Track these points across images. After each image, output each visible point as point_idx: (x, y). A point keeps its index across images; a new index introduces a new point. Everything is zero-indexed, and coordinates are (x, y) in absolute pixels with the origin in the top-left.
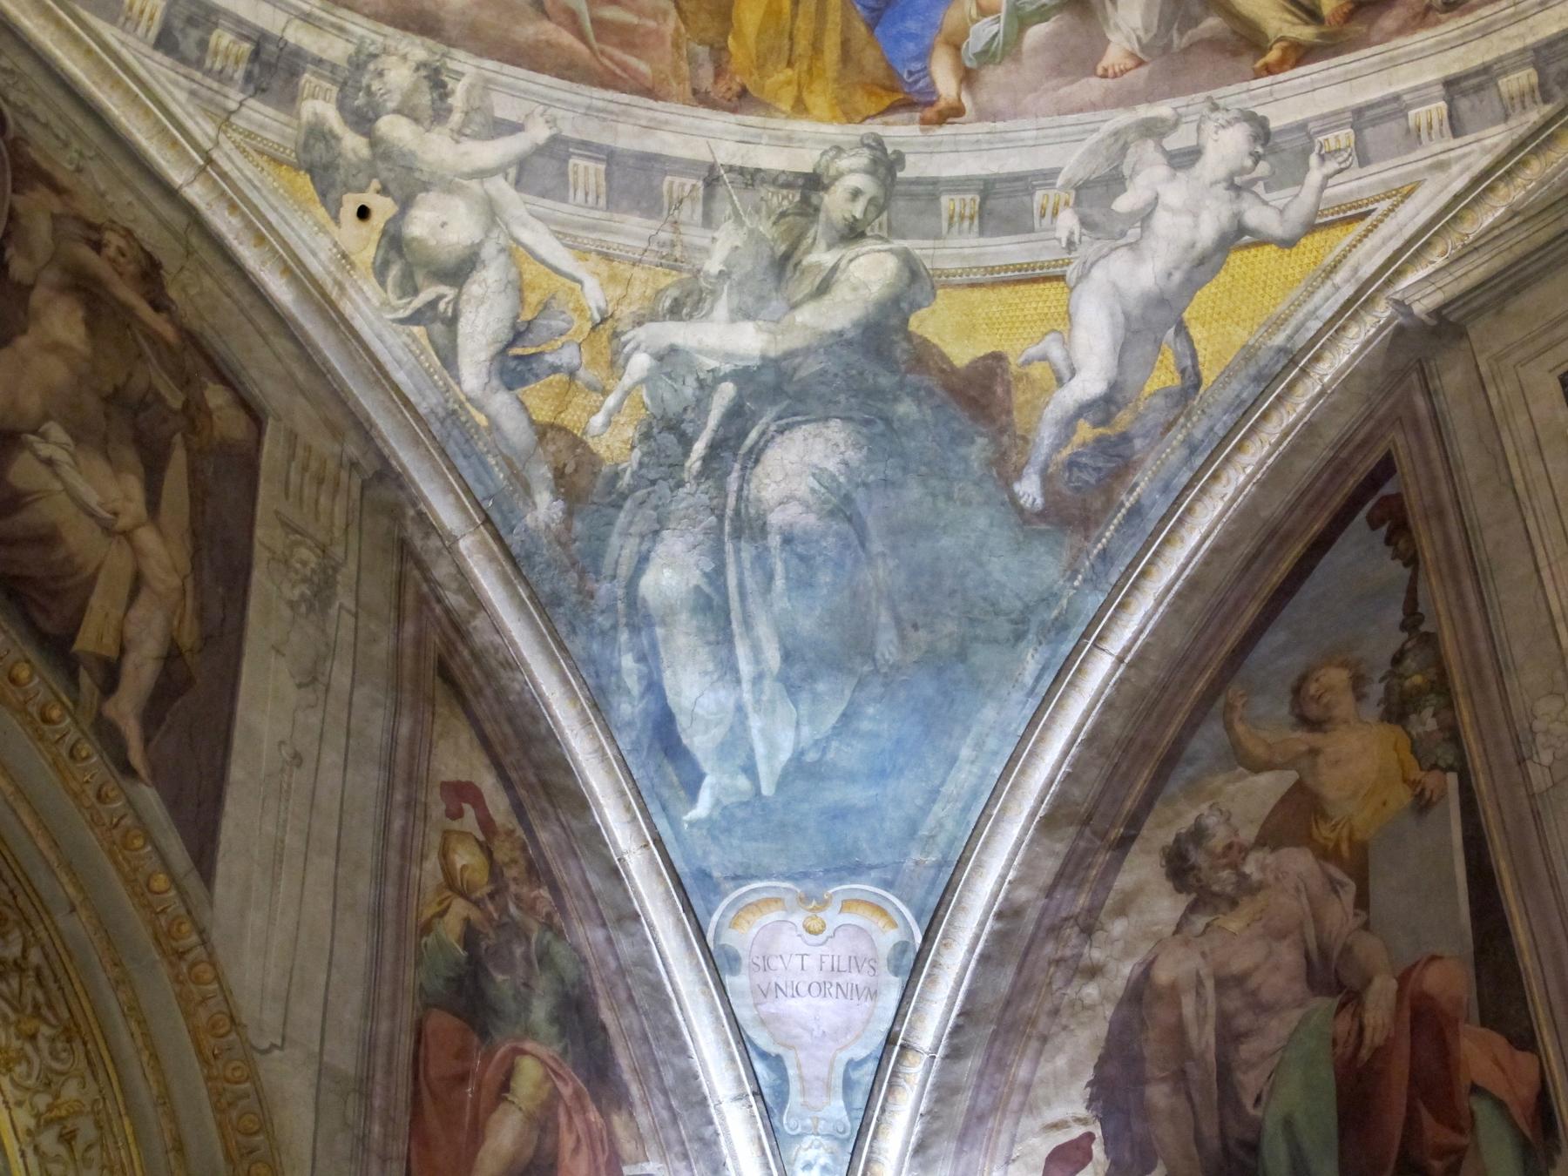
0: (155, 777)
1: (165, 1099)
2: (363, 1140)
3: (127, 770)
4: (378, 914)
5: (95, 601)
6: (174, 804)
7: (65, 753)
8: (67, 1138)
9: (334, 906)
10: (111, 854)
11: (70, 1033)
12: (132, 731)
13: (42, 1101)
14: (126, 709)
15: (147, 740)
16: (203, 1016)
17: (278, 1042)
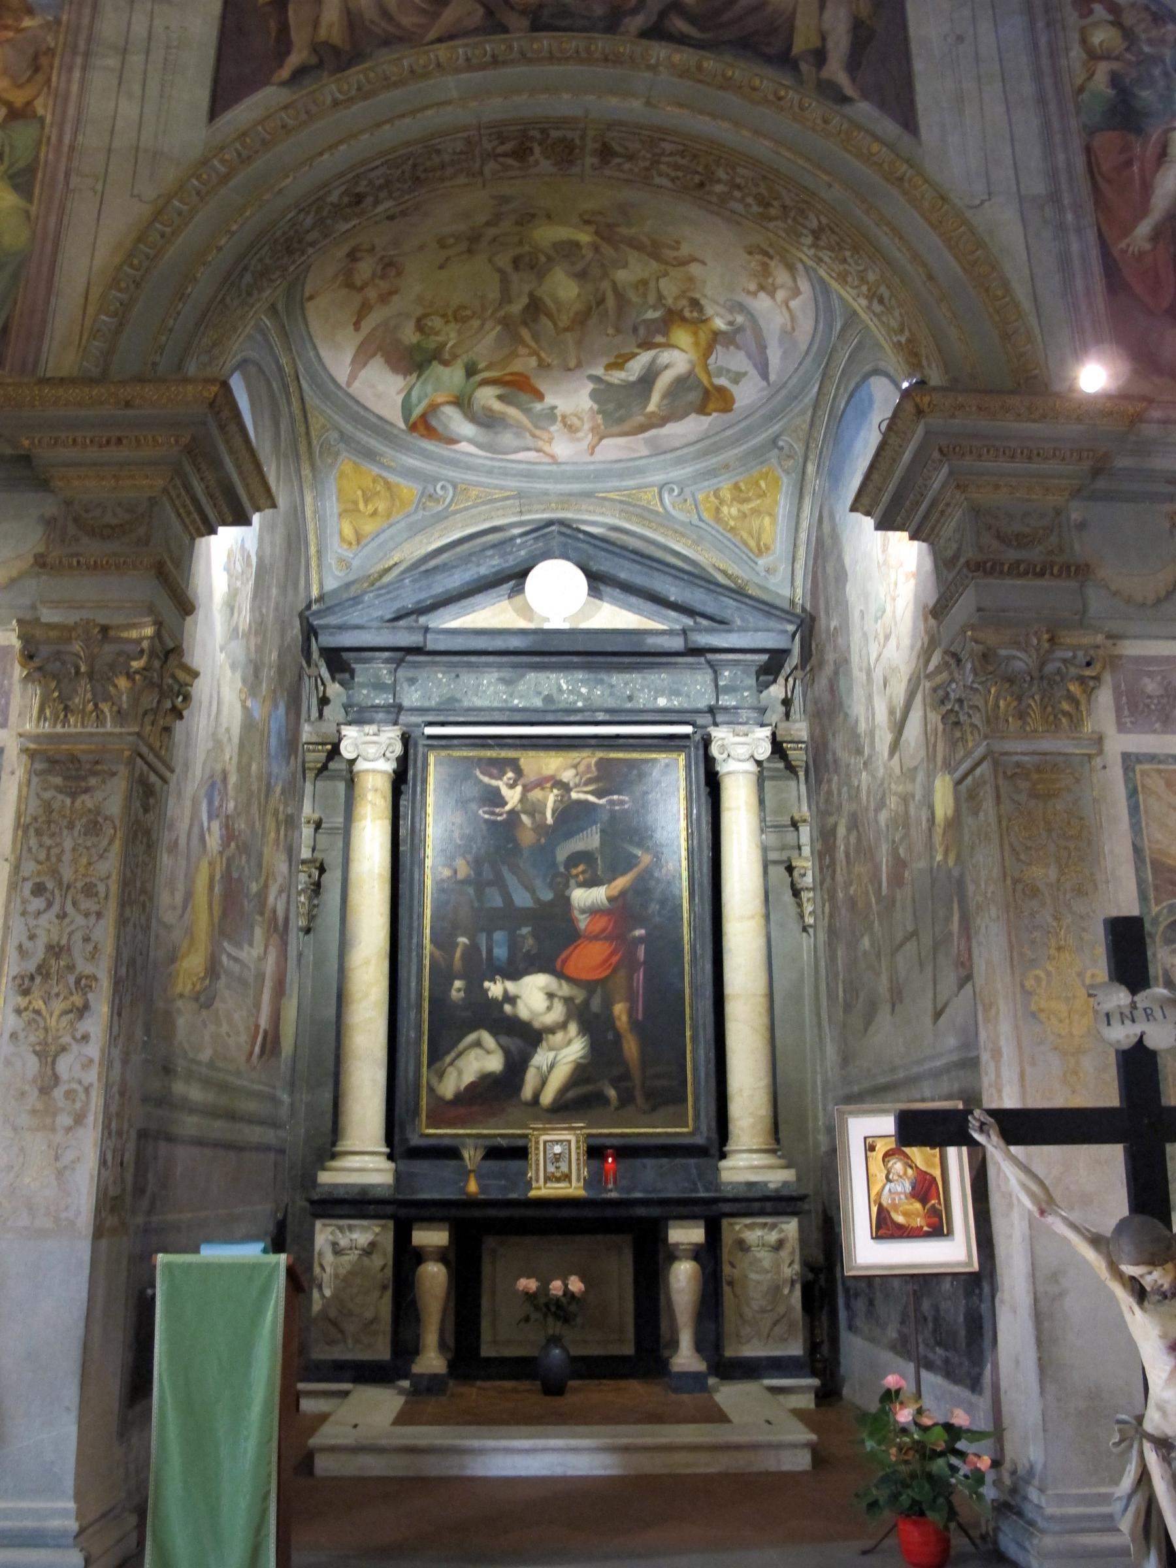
0: (865, 96)
1: (916, 257)
2: (1061, 227)
3: (845, 100)
4: (1042, 100)
5: (799, 23)
6: (882, 104)
7: (797, 110)
8: (881, 301)
9: (1008, 110)
10: (845, 149)
11: (856, 249)
12: (842, 79)
13: (864, 288)
14: (836, 70)
15: (853, 80)
16: (926, 204)
17: (986, 197)
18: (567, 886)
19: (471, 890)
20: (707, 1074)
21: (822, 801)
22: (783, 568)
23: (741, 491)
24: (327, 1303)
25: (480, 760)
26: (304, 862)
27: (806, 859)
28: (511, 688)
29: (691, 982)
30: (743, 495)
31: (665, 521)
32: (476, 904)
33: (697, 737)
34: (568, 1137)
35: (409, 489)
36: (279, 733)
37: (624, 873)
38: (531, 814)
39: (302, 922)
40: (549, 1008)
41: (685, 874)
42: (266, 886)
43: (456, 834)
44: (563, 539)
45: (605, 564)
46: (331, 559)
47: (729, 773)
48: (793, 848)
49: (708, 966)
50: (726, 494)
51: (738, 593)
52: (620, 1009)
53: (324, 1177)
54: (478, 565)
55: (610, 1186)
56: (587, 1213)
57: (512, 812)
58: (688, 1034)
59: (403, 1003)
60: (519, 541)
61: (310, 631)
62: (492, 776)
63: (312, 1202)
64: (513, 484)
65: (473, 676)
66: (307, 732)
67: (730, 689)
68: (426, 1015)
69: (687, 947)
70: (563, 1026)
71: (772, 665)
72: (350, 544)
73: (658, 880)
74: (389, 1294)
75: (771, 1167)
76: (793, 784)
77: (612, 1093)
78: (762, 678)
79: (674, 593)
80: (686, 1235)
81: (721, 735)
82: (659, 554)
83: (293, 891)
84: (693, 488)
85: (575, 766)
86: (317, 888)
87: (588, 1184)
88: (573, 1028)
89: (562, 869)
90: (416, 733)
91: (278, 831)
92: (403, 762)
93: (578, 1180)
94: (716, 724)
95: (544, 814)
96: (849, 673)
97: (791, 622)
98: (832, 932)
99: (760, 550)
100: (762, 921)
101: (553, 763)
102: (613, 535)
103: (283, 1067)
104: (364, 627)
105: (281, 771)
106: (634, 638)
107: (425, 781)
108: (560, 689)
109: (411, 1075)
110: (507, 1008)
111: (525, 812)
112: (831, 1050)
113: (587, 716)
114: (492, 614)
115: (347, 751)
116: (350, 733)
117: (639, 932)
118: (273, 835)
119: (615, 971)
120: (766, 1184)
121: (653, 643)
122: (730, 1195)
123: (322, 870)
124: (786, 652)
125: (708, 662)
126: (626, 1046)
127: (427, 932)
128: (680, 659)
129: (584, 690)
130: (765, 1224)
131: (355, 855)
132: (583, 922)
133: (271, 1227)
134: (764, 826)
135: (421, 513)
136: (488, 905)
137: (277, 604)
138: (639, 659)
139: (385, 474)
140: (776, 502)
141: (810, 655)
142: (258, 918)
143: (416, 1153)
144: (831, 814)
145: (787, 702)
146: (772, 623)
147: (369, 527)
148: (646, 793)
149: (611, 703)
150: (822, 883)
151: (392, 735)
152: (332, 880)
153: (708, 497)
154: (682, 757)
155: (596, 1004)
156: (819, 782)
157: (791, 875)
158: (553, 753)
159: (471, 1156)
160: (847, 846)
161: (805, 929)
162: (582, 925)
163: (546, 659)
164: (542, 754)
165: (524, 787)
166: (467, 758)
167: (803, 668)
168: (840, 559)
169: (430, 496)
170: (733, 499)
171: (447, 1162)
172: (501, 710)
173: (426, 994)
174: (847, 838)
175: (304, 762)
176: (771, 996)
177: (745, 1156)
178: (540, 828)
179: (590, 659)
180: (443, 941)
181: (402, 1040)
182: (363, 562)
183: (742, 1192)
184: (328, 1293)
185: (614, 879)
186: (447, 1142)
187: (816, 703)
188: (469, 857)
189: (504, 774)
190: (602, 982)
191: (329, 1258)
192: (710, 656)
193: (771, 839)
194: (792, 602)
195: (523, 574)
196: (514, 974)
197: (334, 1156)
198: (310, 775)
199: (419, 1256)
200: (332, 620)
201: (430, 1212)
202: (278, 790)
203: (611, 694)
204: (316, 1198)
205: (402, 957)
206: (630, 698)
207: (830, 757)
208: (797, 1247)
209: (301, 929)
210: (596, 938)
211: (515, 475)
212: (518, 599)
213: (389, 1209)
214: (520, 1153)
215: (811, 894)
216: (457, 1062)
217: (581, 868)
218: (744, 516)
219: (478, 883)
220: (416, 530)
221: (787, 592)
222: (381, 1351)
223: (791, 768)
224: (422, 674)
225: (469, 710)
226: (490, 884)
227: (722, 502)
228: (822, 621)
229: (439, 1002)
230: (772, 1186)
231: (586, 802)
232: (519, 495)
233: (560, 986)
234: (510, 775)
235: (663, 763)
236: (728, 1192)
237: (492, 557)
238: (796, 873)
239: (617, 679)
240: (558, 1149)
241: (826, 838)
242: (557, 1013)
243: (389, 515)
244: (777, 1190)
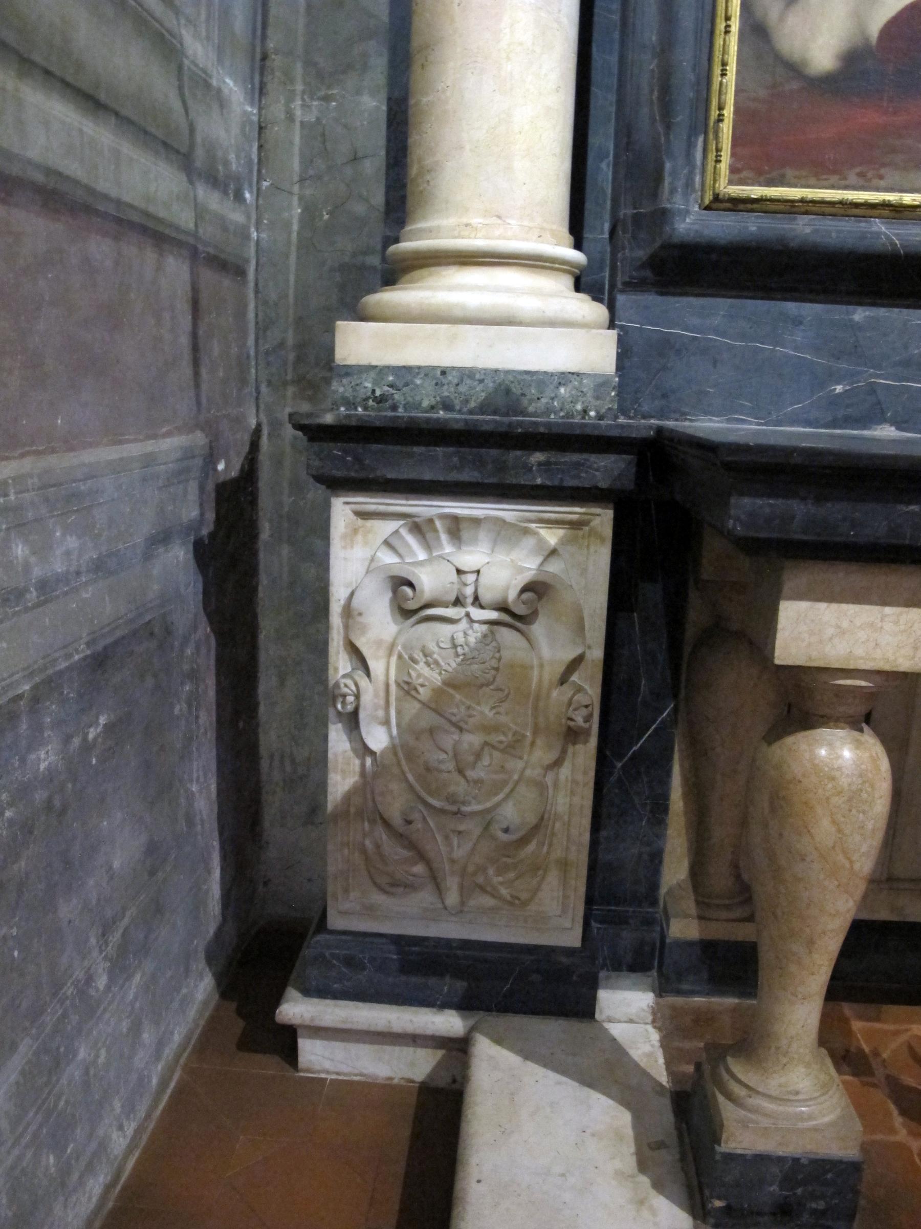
24: (376, 773)
53: (361, 344)
63: (316, 433)
74: (585, 755)
133: (192, 509)
143: (687, 269)
171: (792, 307)
184: (378, 738)
191: (380, 625)
197: (393, 273)
204: (329, 419)
213: (605, 469)
222: (555, 918)
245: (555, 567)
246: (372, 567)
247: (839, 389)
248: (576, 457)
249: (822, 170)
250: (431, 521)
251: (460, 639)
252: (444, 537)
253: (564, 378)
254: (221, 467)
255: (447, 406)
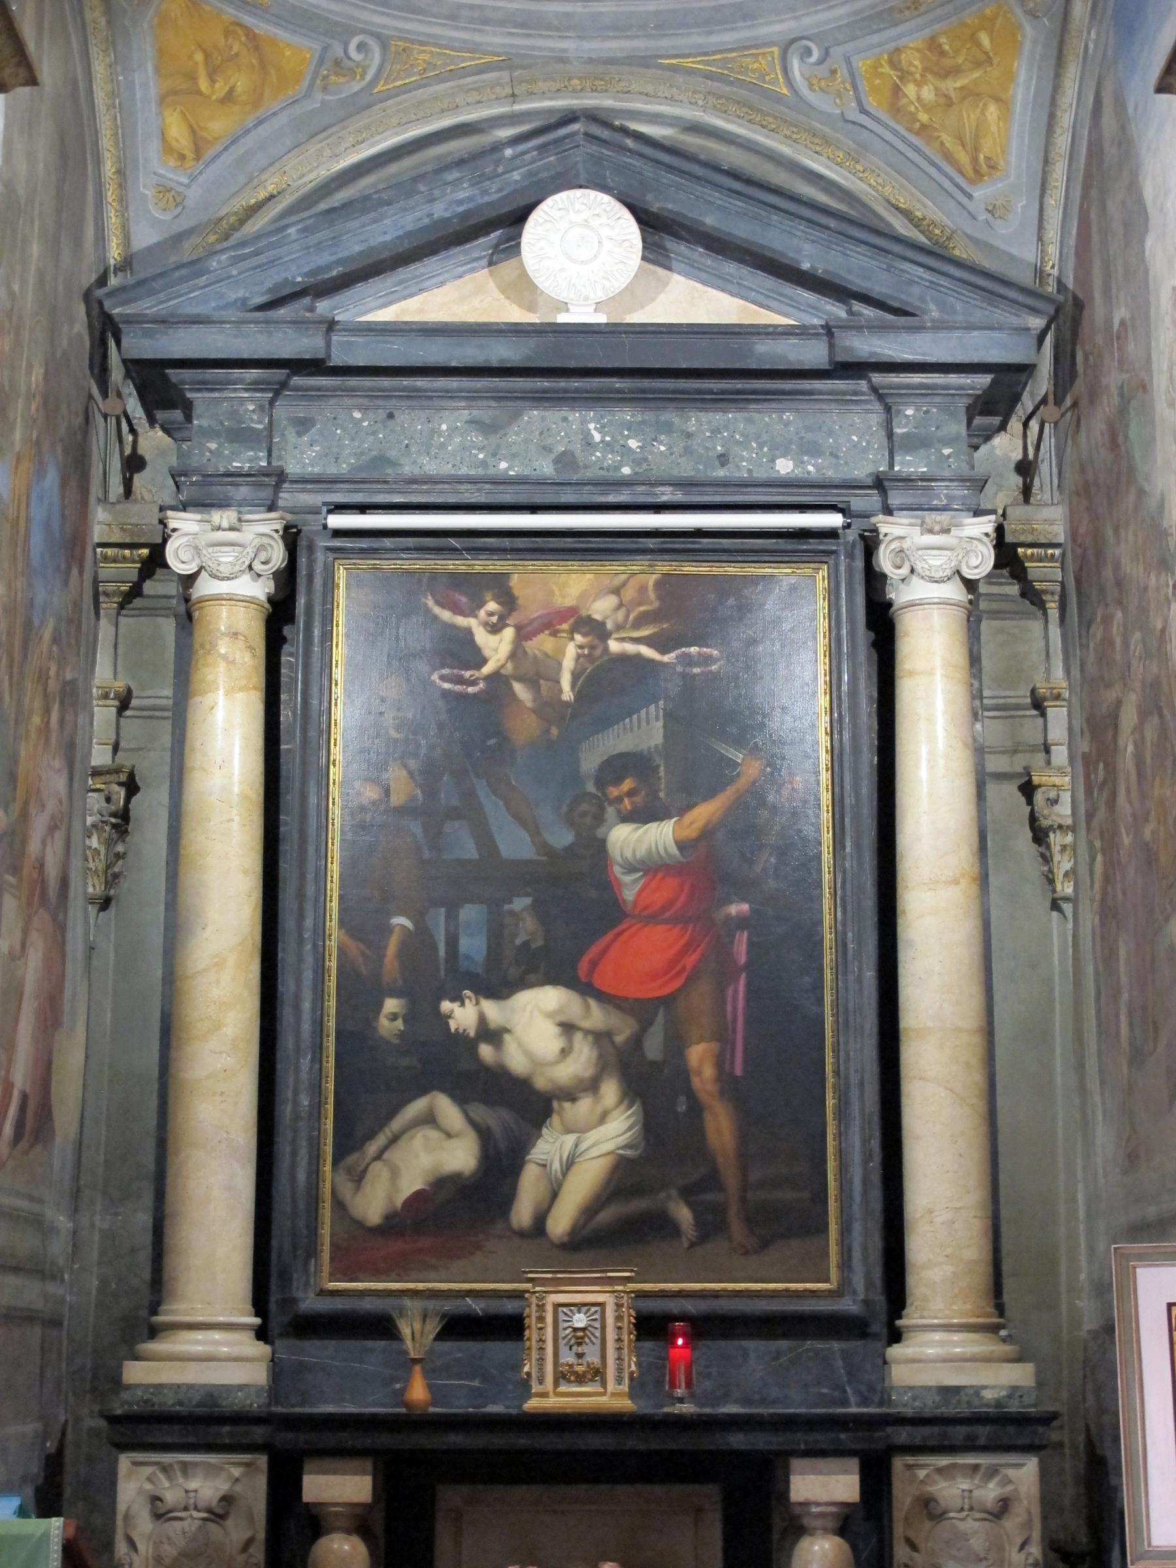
18: (599, 819)
19: (416, 827)
20: (865, 1181)
21: (1091, 657)
22: (1023, 205)
23: (943, 53)
25: (434, 576)
26: (96, 773)
27: (1061, 771)
28: (494, 439)
29: (836, 1004)
30: (947, 62)
31: (792, 114)
32: (427, 854)
33: (852, 536)
34: (600, 1298)
35: (296, 49)
36: (47, 524)
37: (711, 794)
38: (532, 682)
39: (95, 887)
40: (565, 1052)
41: (826, 798)
42: (24, 816)
43: (389, 720)
44: (594, 148)
45: (672, 200)
46: (145, 187)
47: (912, 605)
48: (1033, 749)
49: (870, 975)
50: (913, 60)
51: (934, 253)
52: (700, 1056)
53: (136, 1373)
54: (432, 200)
55: (680, 1392)
56: (633, 1442)
57: (496, 677)
58: (830, 1102)
59: (286, 1042)
60: (508, 152)
61: (106, 328)
62: (457, 610)
63: (113, 1420)
64: (496, 39)
65: (424, 414)
66: (102, 523)
67: (917, 443)
68: (330, 1065)
69: (828, 938)
70: (592, 1086)
71: (998, 397)
72: (182, 157)
73: (774, 809)
75: (988, 1359)
76: (1036, 626)
77: (683, 1214)
78: (978, 421)
79: (809, 255)
80: (821, 1485)
81: (897, 530)
82: (780, 178)
83: (77, 827)
84: (849, 47)
85: (617, 591)
86: (122, 822)
87: (637, 1387)
88: (610, 1091)
89: (591, 788)
90: (311, 525)
91: (47, 711)
92: (287, 581)
93: (619, 1380)
94: (888, 511)
95: (558, 682)
96: (1147, 411)
97: (1035, 311)
98: (1108, 912)
99: (977, 171)
100: (974, 889)
101: (574, 585)
102: (692, 142)
103: (57, 1164)
104: (209, 320)
105: (52, 598)
106: (735, 342)
107: (328, 619)
108: (589, 443)
109: (301, 1176)
110: (486, 1051)
111: (520, 679)
112: (1104, 1138)
113: (640, 495)
114: (456, 297)
115: (179, 558)
116: (185, 524)
117: (737, 909)
118: (36, 720)
119: (692, 979)
120: (977, 1390)
121: (766, 352)
122: (908, 1411)
123: (132, 787)
124: (1025, 370)
125: (874, 389)
126: (710, 1124)
127: (334, 906)
128: (817, 384)
129: (633, 444)
130: (976, 1468)
131: (195, 760)
132: (630, 888)
133: (35, 1468)
134: (978, 705)
135: (319, 96)
136: (446, 856)
137: (41, 275)
138: (739, 384)
139: (248, 20)
140: (1010, 76)
141: (1073, 375)
142: (10, 879)
143: (310, 1326)
144: (1109, 686)
145: (1025, 468)
146: (1000, 315)
147: (218, 125)
148: (753, 642)
149: (686, 469)
150: (1090, 816)
151: (265, 529)
152: (151, 805)
153: (877, 65)
154: (824, 572)
155: (654, 1047)
156: (1086, 623)
157: (1030, 801)
158: (574, 565)
159: (416, 1332)
160: (1139, 745)
161: (1055, 905)
162: (629, 895)
163: (562, 383)
164: (553, 566)
165: (519, 628)
166: (408, 573)
167: (1058, 402)
168: (1134, 188)
169: (337, 63)
170: (925, 70)
171: (369, 1344)
172: (472, 480)
173: (331, 1024)
174: (1139, 729)
175: (96, 582)
176: (989, 1031)
177: (937, 1336)
178: (549, 708)
179: (646, 383)
180: (364, 924)
181: (285, 1112)
182: (209, 191)
183: (930, 1406)
185: (690, 807)
186: (368, 1305)
187: (1083, 470)
188: (413, 764)
189: (482, 604)
190: (668, 1001)
191: (144, 1525)
192: (877, 378)
193: (993, 730)
194: (1040, 274)
195: (519, 217)
196: (498, 987)
197: (154, 1332)
198: (108, 606)
199: (315, 1523)
200: (147, 306)
201: (339, 1438)
202: (47, 635)
203: (688, 451)
204: (119, 1412)
205: (286, 955)
206: (723, 459)
207: (1108, 573)
208: (1036, 1510)
209: (91, 900)
210: (652, 918)
211: (501, 23)
212: (507, 268)
213: (259, 1433)
214: (511, 1327)
215: (1069, 839)
216: (386, 1156)
217: (627, 785)
218: (949, 103)
219: (429, 812)
220: (314, 129)
221: (1029, 254)
223: (1032, 596)
224: (323, 412)
225: (413, 481)
226: (453, 814)
227: (904, 75)
228: (1097, 311)
229: (355, 1039)
230: (988, 1395)
231: (638, 656)
232: (509, 62)
233: (587, 1008)
234: (492, 606)
235: (785, 584)
236: (904, 1405)
237: (455, 183)
238: (1039, 798)
239: (698, 422)
240: (580, 1320)
241: (1099, 729)
242: (581, 1061)
243: (257, 103)
244: (998, 1404)
245: (238, 1488)
246: (141, 1491)
247: (398, 1386)
248: (245, 1428)
249: (377, 1273)
250: (171, 1465)
251: (187, 1529)
252: (179, 1473)
253: (241, 1387)
254: (48, 1445)
255: (181, 1404)
